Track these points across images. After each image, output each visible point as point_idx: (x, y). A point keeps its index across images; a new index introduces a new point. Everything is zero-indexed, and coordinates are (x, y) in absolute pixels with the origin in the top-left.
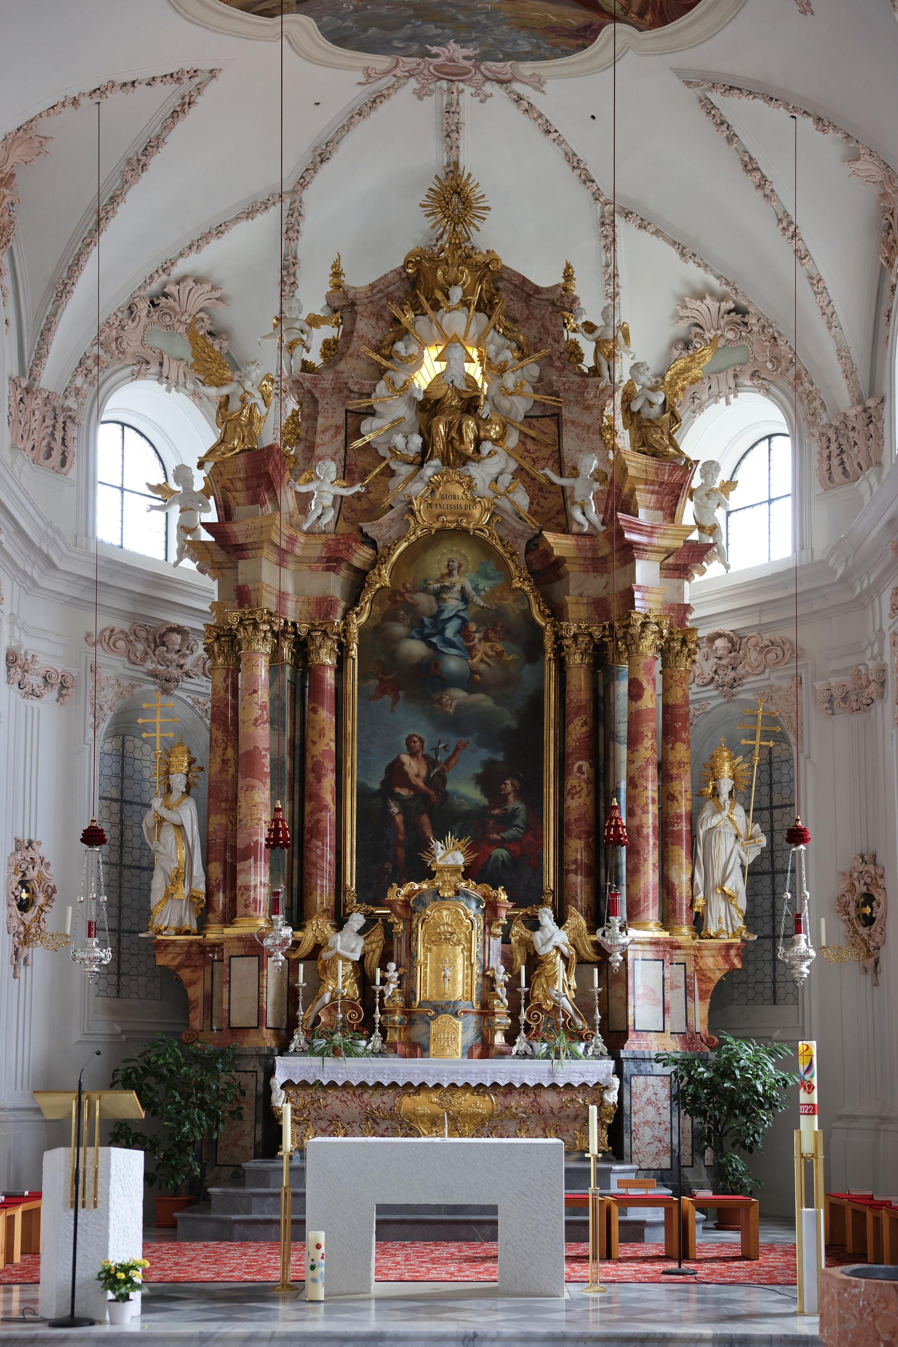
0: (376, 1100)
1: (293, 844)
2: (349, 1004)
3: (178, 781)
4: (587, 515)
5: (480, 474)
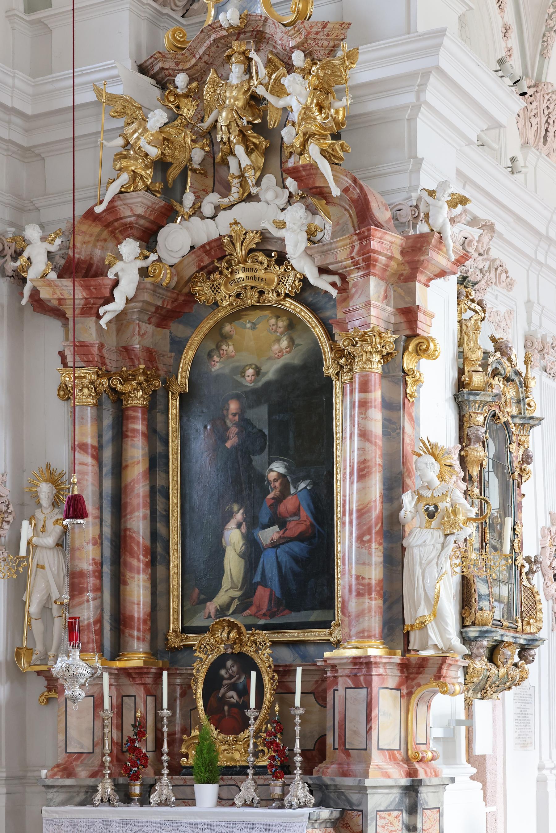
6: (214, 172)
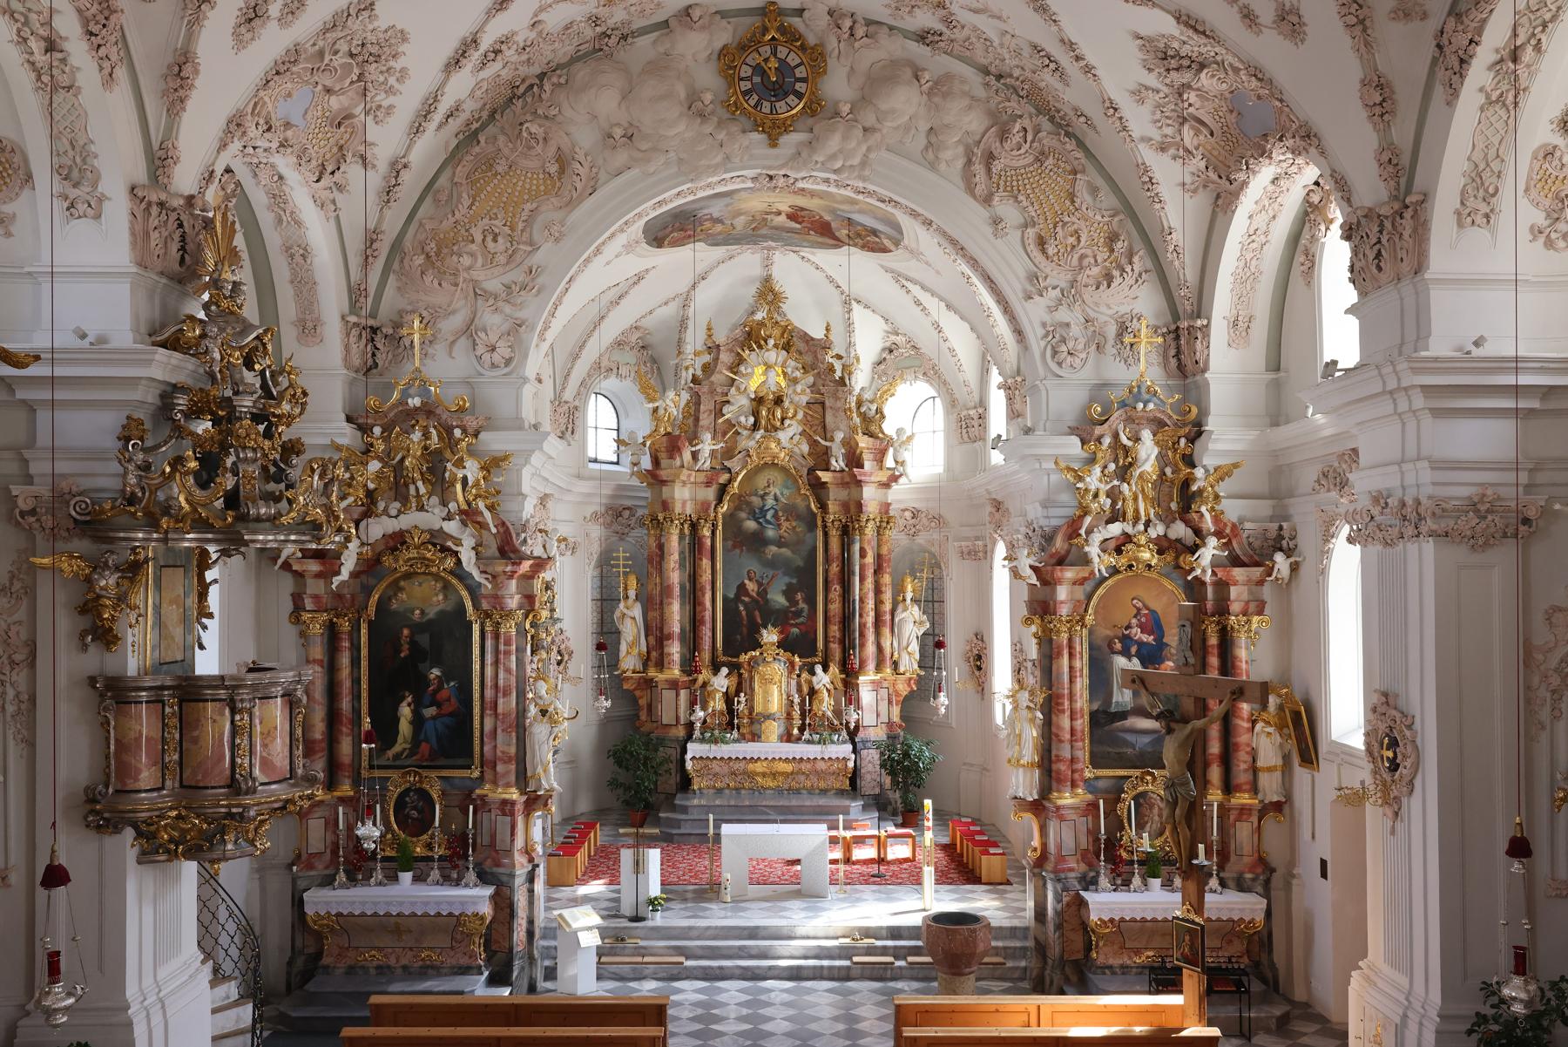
0: (736, 766)
1: (692, 640)
2: (722, 713)
3: (632, 593)
4: (838, 463)
5: (783, 436)
6: (398, 487)
